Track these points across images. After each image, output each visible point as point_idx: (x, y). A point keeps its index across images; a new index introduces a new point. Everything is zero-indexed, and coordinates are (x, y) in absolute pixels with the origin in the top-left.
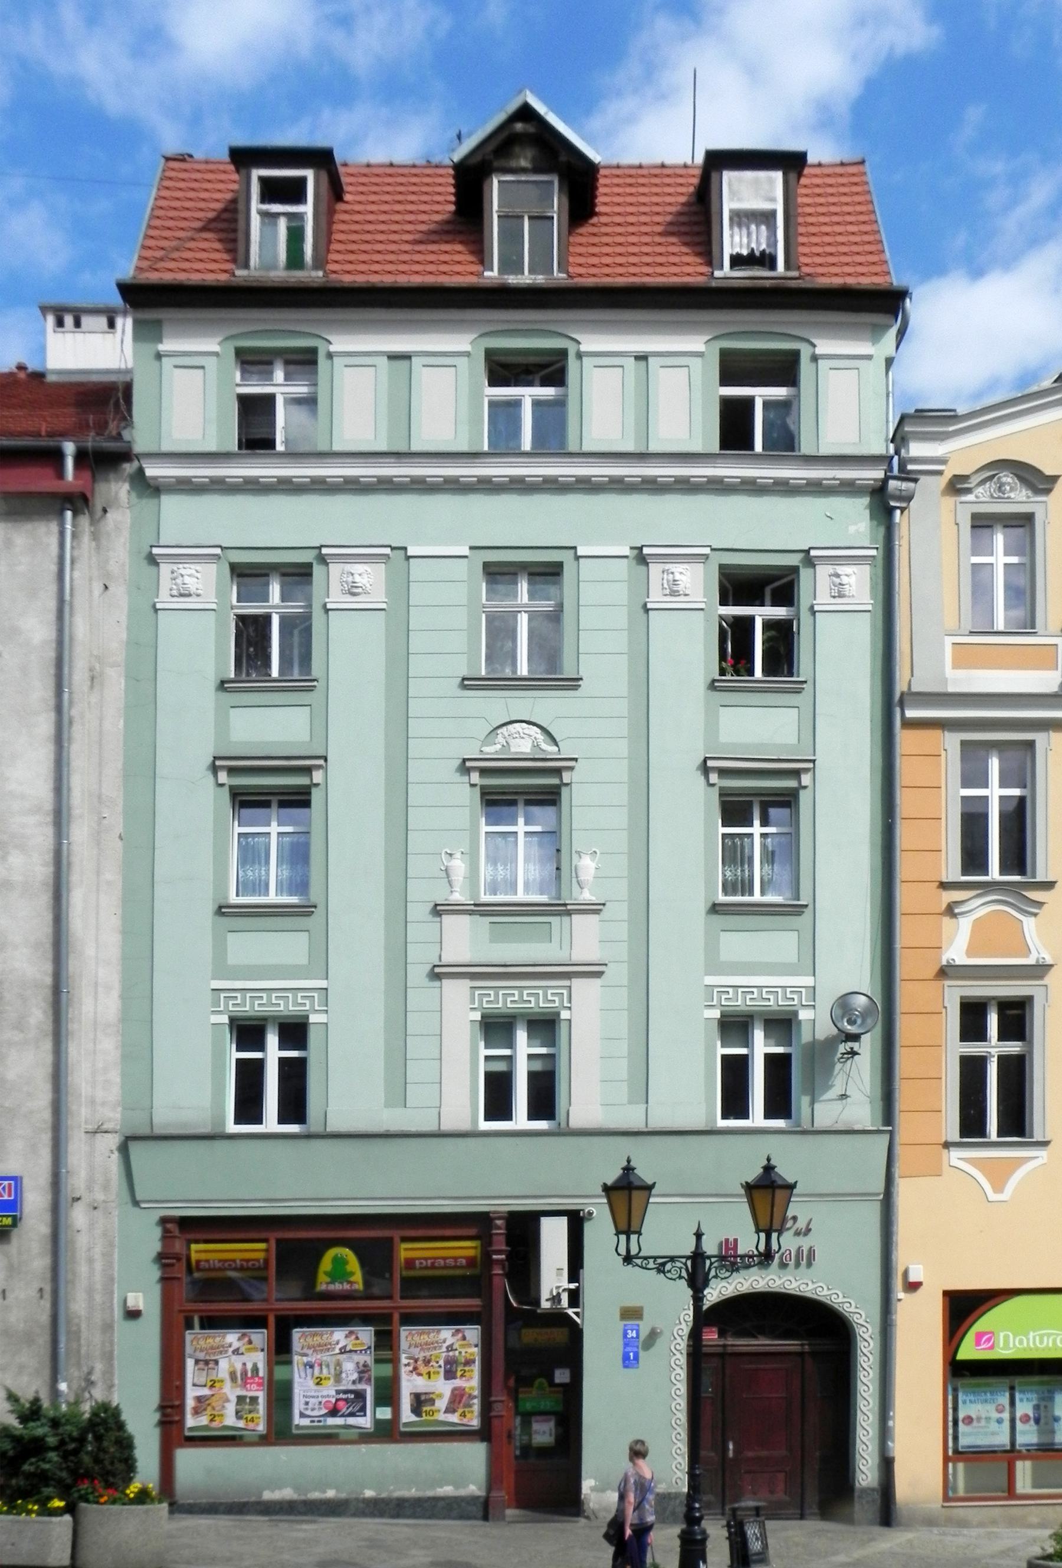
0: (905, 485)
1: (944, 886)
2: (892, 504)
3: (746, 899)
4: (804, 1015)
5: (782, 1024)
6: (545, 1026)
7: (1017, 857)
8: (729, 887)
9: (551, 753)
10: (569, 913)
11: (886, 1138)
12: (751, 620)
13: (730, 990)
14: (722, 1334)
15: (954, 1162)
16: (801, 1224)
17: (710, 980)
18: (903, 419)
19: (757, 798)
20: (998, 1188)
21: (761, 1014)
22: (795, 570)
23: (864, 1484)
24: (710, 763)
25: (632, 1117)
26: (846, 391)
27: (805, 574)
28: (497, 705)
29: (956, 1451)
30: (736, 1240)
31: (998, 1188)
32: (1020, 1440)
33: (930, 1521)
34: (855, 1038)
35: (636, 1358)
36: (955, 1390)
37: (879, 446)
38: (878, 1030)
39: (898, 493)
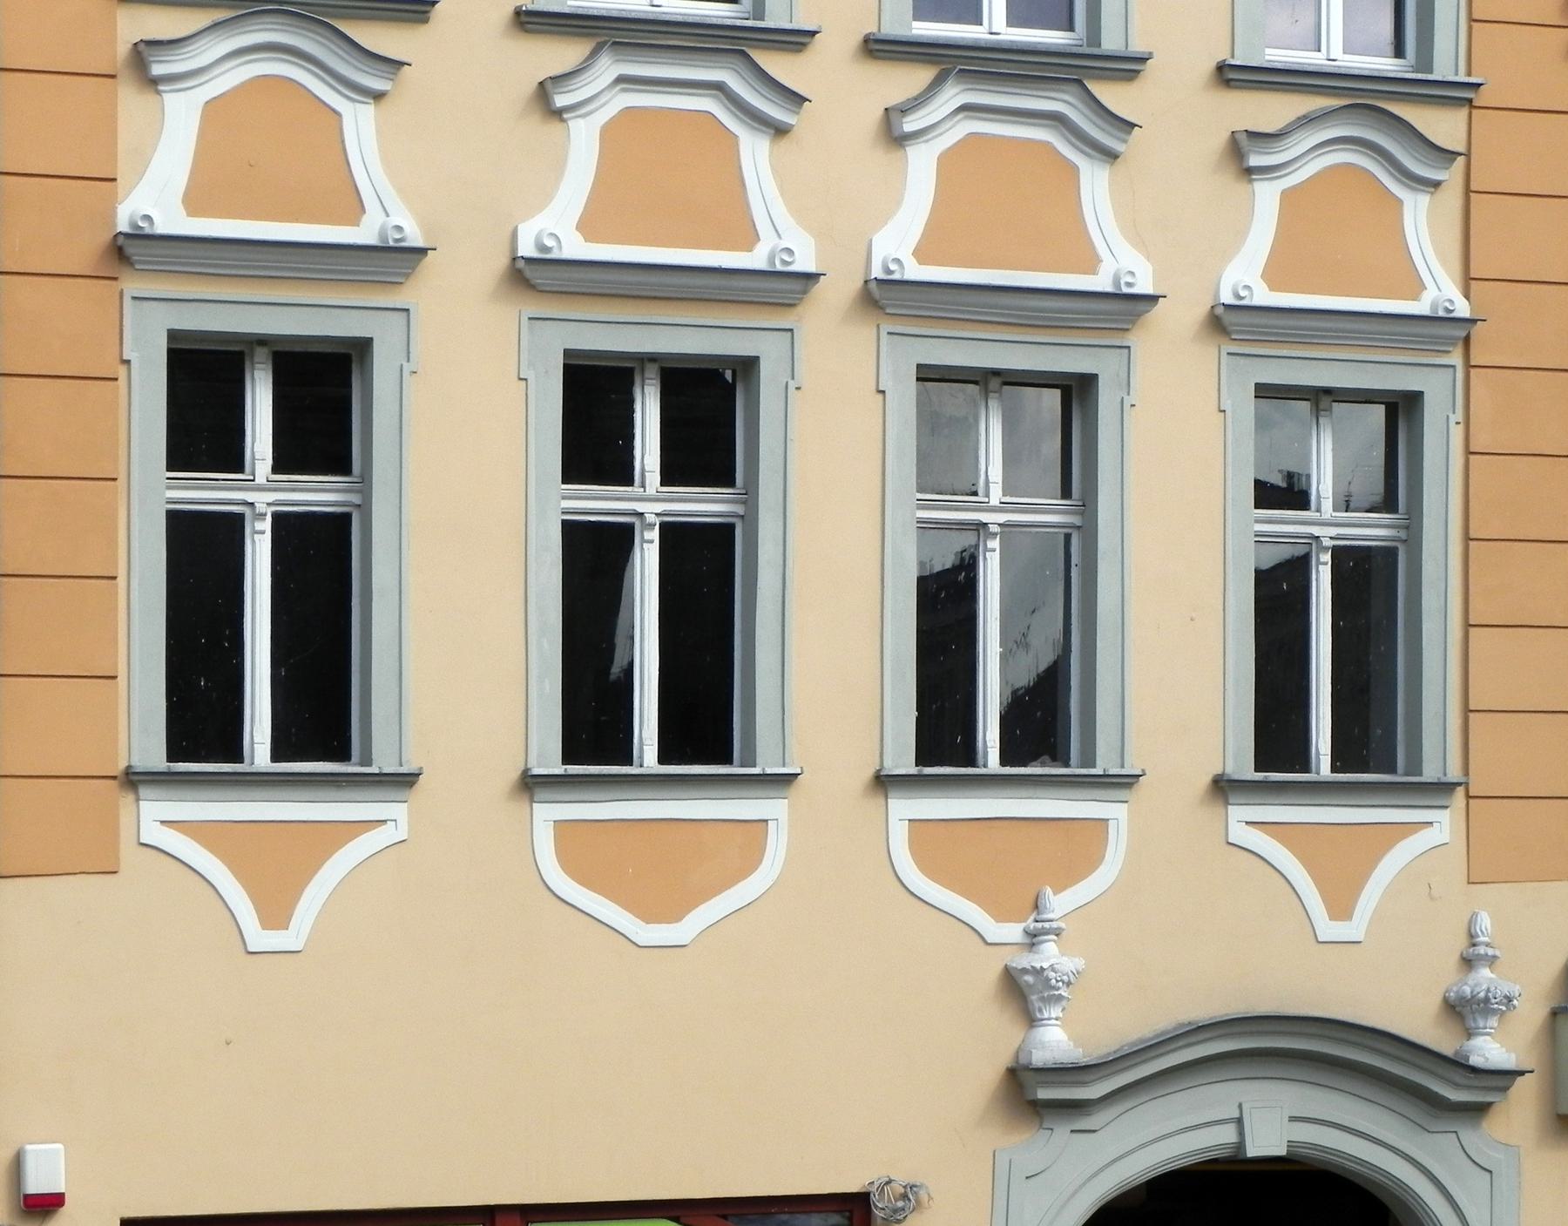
15: (154, 833)
20: (275, 914)
31: (275, 914)
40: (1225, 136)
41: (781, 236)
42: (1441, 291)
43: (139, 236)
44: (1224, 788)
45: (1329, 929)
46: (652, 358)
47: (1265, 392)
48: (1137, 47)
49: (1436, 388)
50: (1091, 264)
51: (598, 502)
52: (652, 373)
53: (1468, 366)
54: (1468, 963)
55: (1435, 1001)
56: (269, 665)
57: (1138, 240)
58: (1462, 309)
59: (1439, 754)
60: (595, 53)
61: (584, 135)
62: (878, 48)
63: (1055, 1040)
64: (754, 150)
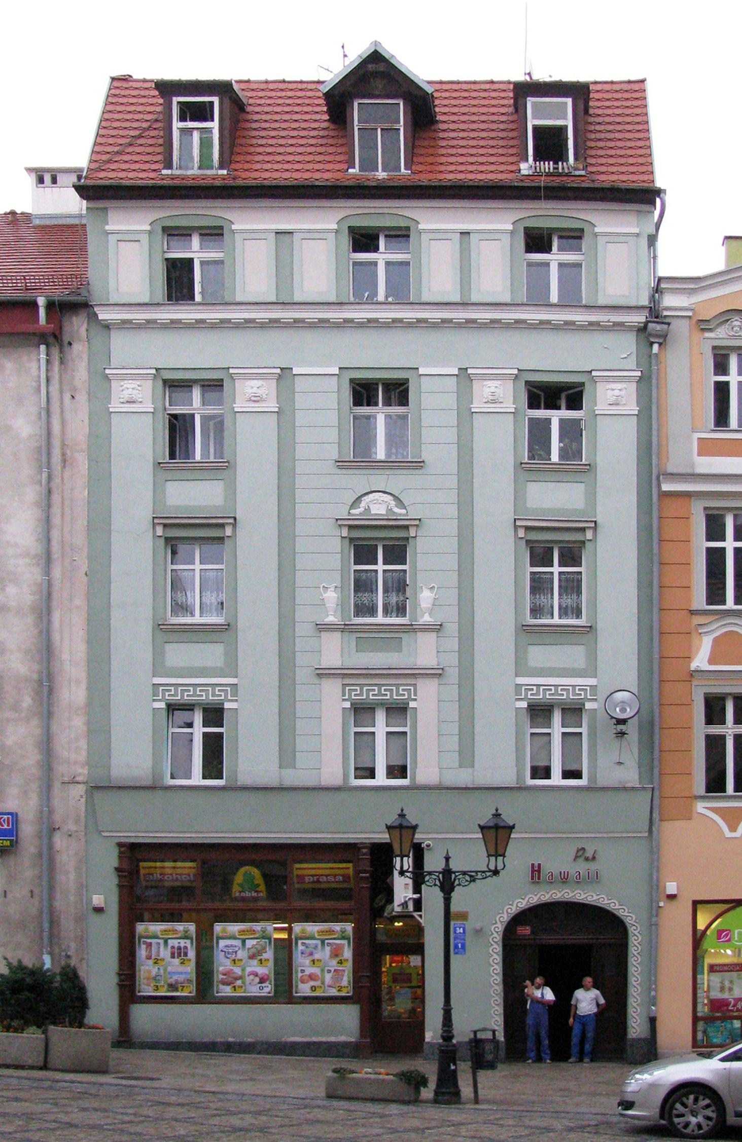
1: (693, 613)
2: (652, 340)
4: (588, 706)
5: (573, 711)
6: (398, 710)
9: (400, 515)
10: (415, 631)
12: (548, 421)
13: (535, 688)
16: (589, 854)
19: (556, 551)
23: (634, 1036)
24: (518, 523)
25: (463, 777)
28: (359, 481)
30: (539, 865)
35: (463, 946)
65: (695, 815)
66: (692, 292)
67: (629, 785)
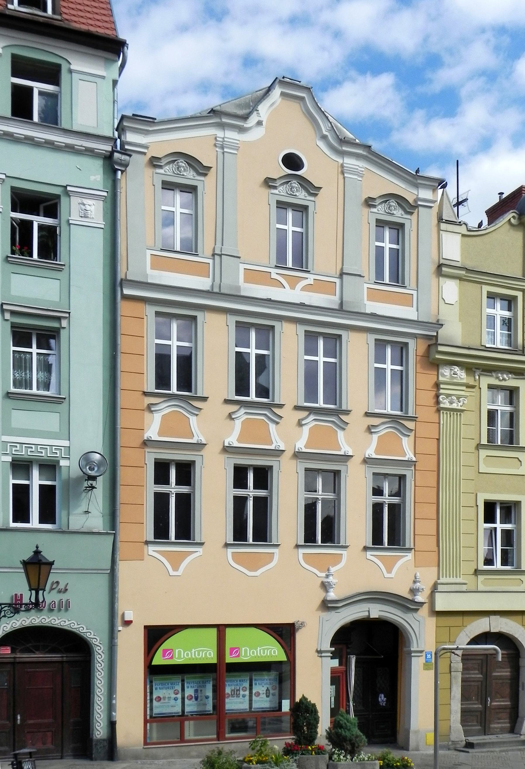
0: (124, 157)
1: (145, 394)
2: (116, 167)
3: (28, 391)
4: (63, 463)
5: (50, 467)
7: (186, 381)
8: (17, 383)
11: (111, 538)
13: (18, 445)
14: (13, 651)
15: (151, 553)
16: (62, 586)
17: (5, 438)
18: (123, 118)
20: (176, 569)
21: (37, 461)
22: (58, 197)
23: (98, 737)
24: (5, 307)
26: (88, 95)
27: (64, 200)
29: (151, 717)
30: (21, 595)
31: (176, 569)
32: (187, 709)
33: (136, 757)
34: (94, 478)
36: (151, 682)
37: (108, 132)
38: (107, 475)
39: (119, 161)
40: (366, 426)
41: (278, 443)
42: (410, 455)
43: (148, 440)
44: (366, 549)
45: (387, 575)
46: (251, 465)
47: (374, 474)
48: (349, 409)
49: (408, 473)
50: (340, 449)
51: (241, 492)
52: (252, 468)
53: (415, 470)
54: (415, 582)
55: (408, 590)
56: (175, 521)
57: (349, 445)
58: (414, 459)
59: (409, 543)
60: (240, 407)
61: (238, 424)
62: (297, 408)
63: (332, 595)
64: (272, 427)
65: (146, 557)
66: (147, 133)
67: (95, 530)
